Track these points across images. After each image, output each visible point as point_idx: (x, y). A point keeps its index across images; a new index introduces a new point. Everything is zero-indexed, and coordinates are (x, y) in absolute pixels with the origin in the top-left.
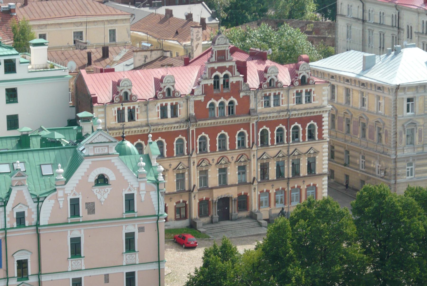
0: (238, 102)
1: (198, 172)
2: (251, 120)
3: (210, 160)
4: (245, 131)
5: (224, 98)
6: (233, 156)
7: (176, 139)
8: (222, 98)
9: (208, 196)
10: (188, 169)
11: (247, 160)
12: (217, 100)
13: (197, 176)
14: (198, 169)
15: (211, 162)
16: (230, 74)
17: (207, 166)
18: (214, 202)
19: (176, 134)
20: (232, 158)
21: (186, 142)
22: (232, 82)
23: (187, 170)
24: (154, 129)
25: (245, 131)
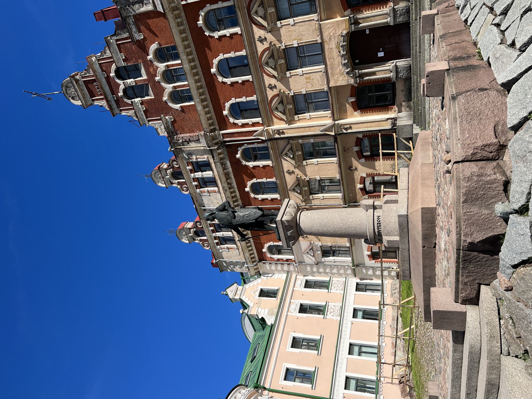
2: (173, 5)
3: (270, 94)
7: (244, 163)
9: (348, 92)
10: (291, 141)
12: (164, 89)
15: (275, 92)
16: (114, 67)
19: (236, 163)
22: (124, 60)
24: (234, 202)
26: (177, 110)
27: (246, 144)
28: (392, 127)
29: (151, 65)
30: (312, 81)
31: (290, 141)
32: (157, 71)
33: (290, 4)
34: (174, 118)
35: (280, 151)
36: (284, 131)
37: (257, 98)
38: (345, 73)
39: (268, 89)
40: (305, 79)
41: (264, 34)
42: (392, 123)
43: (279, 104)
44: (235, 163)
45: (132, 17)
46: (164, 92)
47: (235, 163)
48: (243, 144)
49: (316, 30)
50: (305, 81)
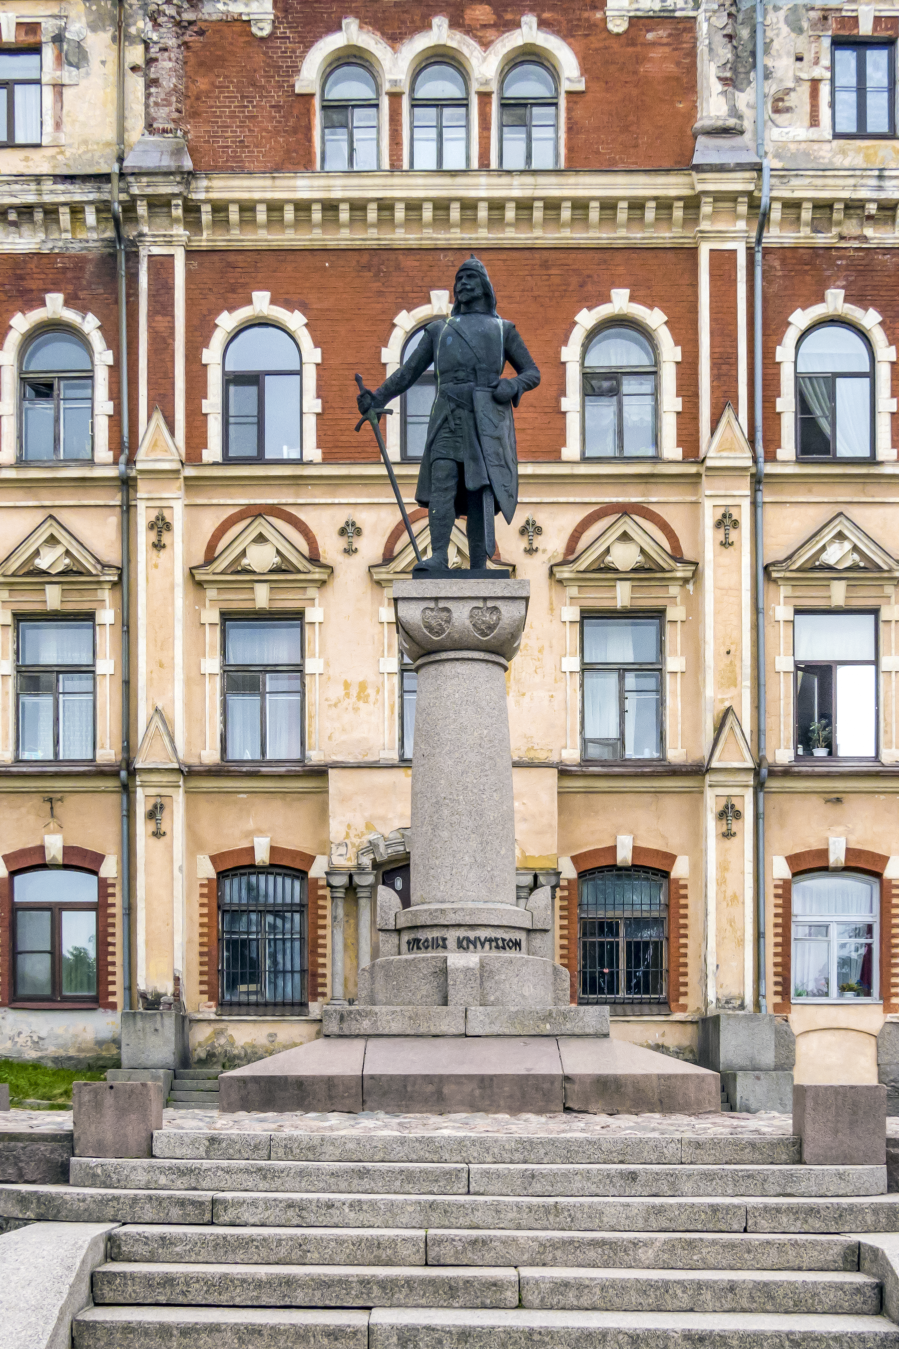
0: (585, 69)
1: (212, 616)
4: (655, 318)
5: (456, 23)
6: (542, 518)
8: (440, 23)
11: (664, 561)
12: (395, 38)
13: (196, 651)
14: (211, 593)
17: (283, 568)
18: (340, 881)
20: (531, 530)
21: (103, 357)
23: (106, 594)
25: (655, 318)
26: (296, 70)
27: (111, 363)
28: (143, 996)
29: (499, 16)
30: (350, 708)
31: (115, 571)
32: (475, 37)
33: (625, 670)
34: (262, 39)
35: (62, 516)
36: (163, 554)
37: (310, 463)
38: (372, 837)
39: (341, 517)
40: (361, 679)
41: (544, 551)
42: (158, 996)
43: (278, 552)
44: (21, 278)
45: (692, 14)
46: (383, 34)
47: (21, 278)
48: (112, 343)
49: (529, 750)
50: (355, 678)
